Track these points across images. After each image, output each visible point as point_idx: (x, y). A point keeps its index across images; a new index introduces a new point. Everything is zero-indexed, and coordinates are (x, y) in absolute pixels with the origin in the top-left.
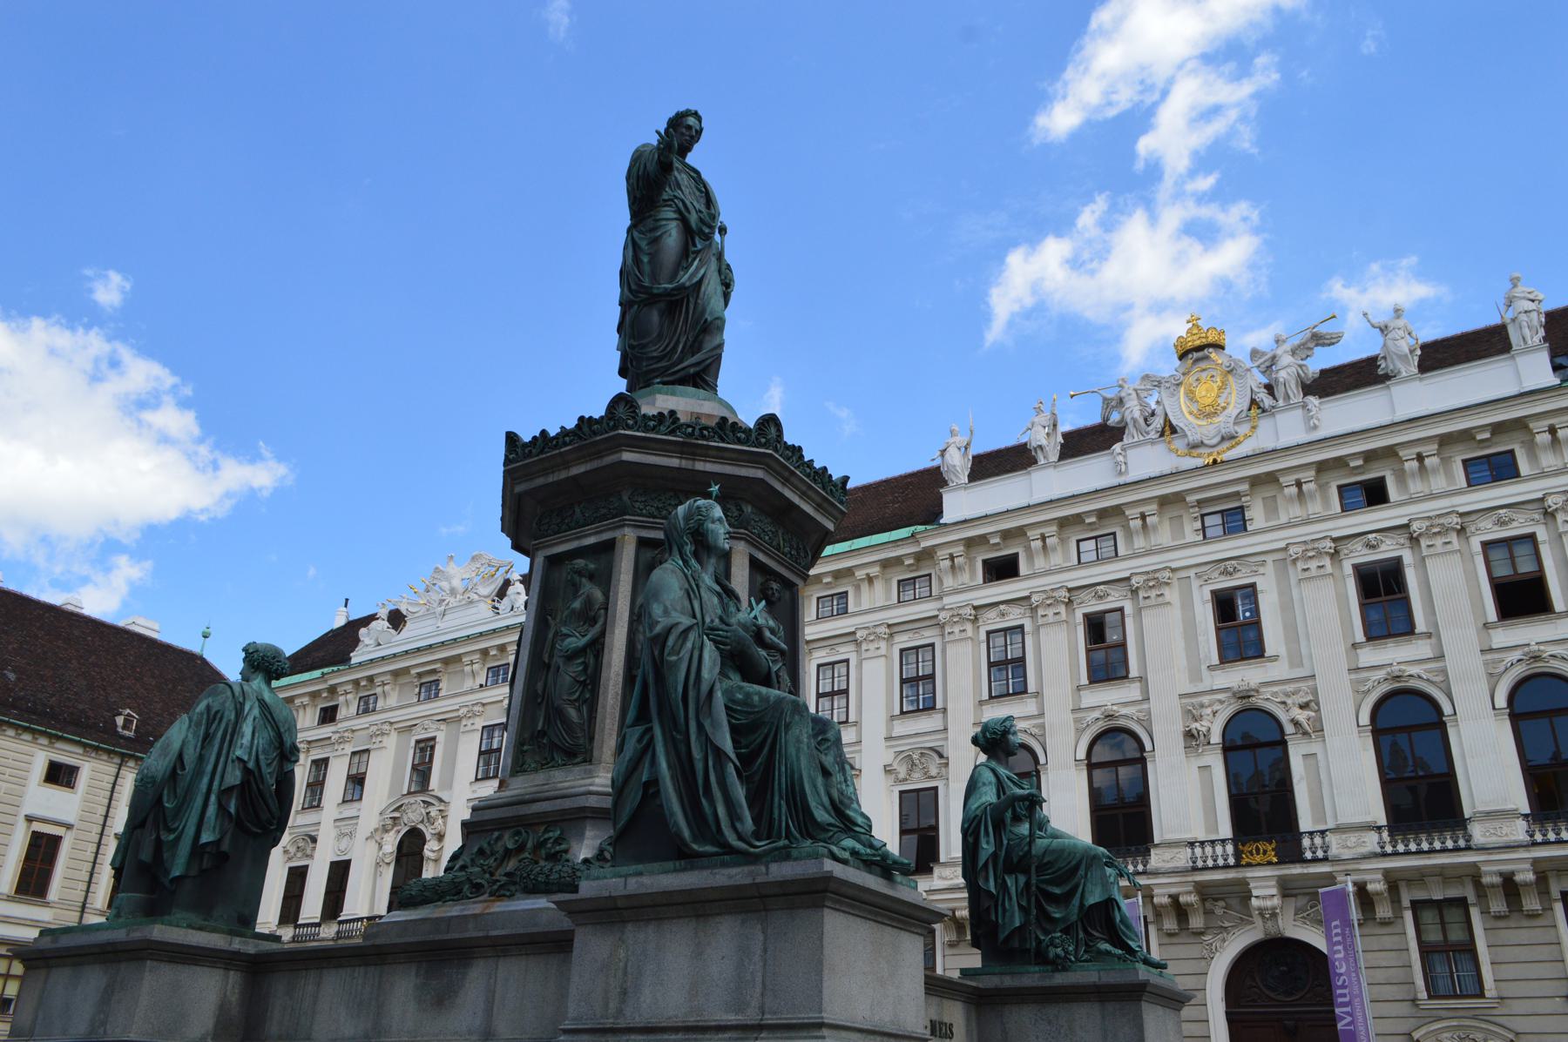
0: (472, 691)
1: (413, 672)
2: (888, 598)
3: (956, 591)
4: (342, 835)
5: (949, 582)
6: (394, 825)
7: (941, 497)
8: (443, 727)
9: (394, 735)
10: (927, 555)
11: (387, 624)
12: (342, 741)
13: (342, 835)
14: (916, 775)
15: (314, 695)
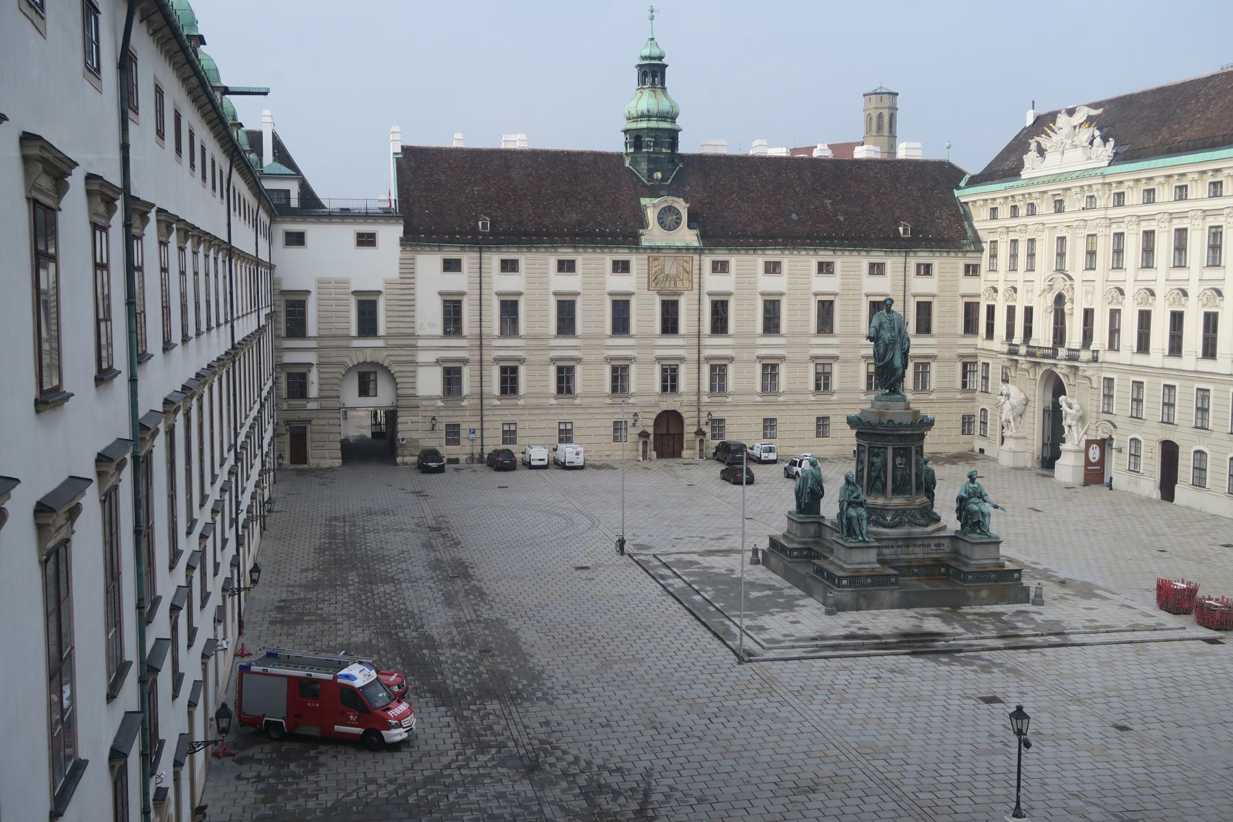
4: (1028, 291)
11: (1036, 154)
13: (1028, 291)
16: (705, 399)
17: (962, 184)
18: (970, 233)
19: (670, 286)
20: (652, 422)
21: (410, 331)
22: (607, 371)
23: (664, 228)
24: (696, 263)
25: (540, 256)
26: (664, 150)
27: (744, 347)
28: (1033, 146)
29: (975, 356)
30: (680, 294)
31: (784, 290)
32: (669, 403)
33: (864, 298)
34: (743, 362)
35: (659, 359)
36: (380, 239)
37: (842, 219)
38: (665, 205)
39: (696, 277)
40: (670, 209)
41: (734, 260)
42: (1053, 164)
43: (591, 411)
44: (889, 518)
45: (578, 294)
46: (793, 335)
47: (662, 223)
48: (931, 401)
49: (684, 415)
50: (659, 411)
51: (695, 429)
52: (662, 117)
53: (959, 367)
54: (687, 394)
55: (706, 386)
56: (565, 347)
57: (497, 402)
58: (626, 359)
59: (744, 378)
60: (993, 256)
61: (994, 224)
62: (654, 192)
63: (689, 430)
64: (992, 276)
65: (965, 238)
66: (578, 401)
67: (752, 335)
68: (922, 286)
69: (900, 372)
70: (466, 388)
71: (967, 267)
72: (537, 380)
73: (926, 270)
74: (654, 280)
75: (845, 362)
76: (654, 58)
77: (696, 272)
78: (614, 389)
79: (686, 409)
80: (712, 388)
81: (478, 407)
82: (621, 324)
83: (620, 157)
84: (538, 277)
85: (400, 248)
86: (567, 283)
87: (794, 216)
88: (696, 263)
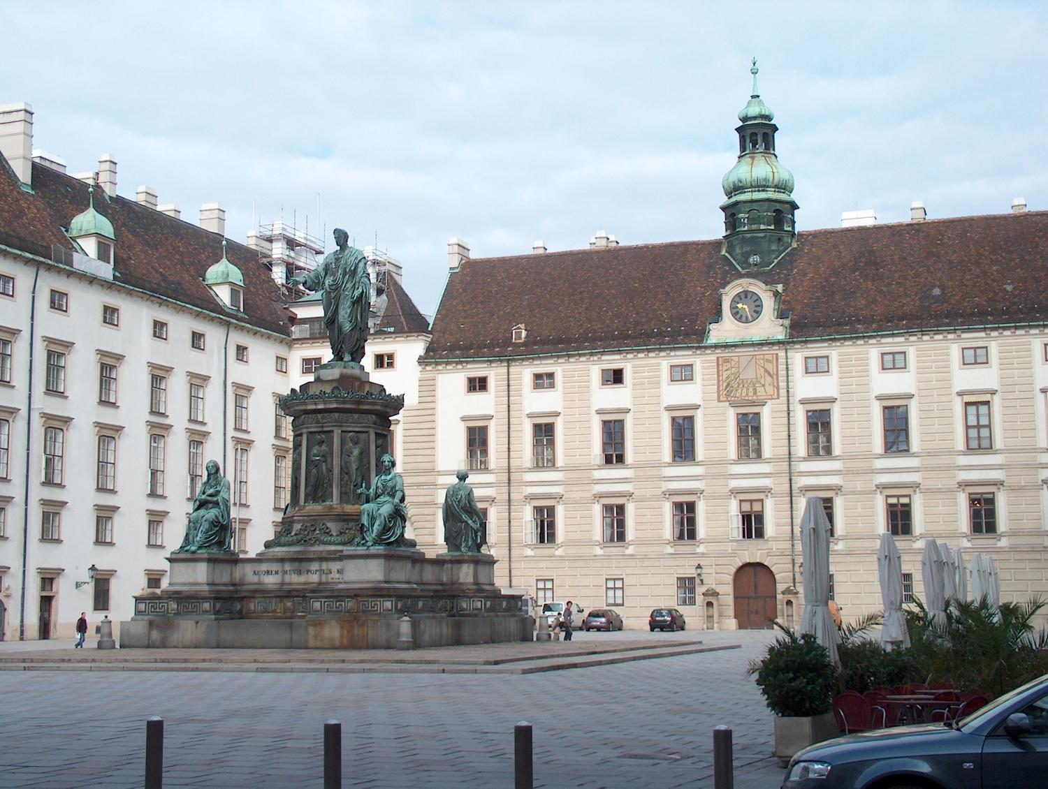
19: (741, 393)
21: (429, 466)
23: (739, 320)
24: (782, 361)
25: (579, 366)
26: (762, 227)
31: (912, 390)
32: (753, 552)
34: (854, 493)
35: (735, 492)
36: (398, 361)
37: (1009, 288)
38: (739, 290)
39: (782, 379)
40: (745, 295)
43: (646, 563)
44: (293, 534)
46: (930, 454)
47: (737, 315)
52: (761, 186)
54: (776, 539)
56: (613, 480)
57: (529, 552)
58: (690, 492)
66: (630, 551)
69: (347, 327)
76: (755, 118)
77: (782, 373)
79: (775, 559)
83: (717, 245)
85: (420, 368)
86: (615, 397)
87: (936, 291)
88: (782, 361)
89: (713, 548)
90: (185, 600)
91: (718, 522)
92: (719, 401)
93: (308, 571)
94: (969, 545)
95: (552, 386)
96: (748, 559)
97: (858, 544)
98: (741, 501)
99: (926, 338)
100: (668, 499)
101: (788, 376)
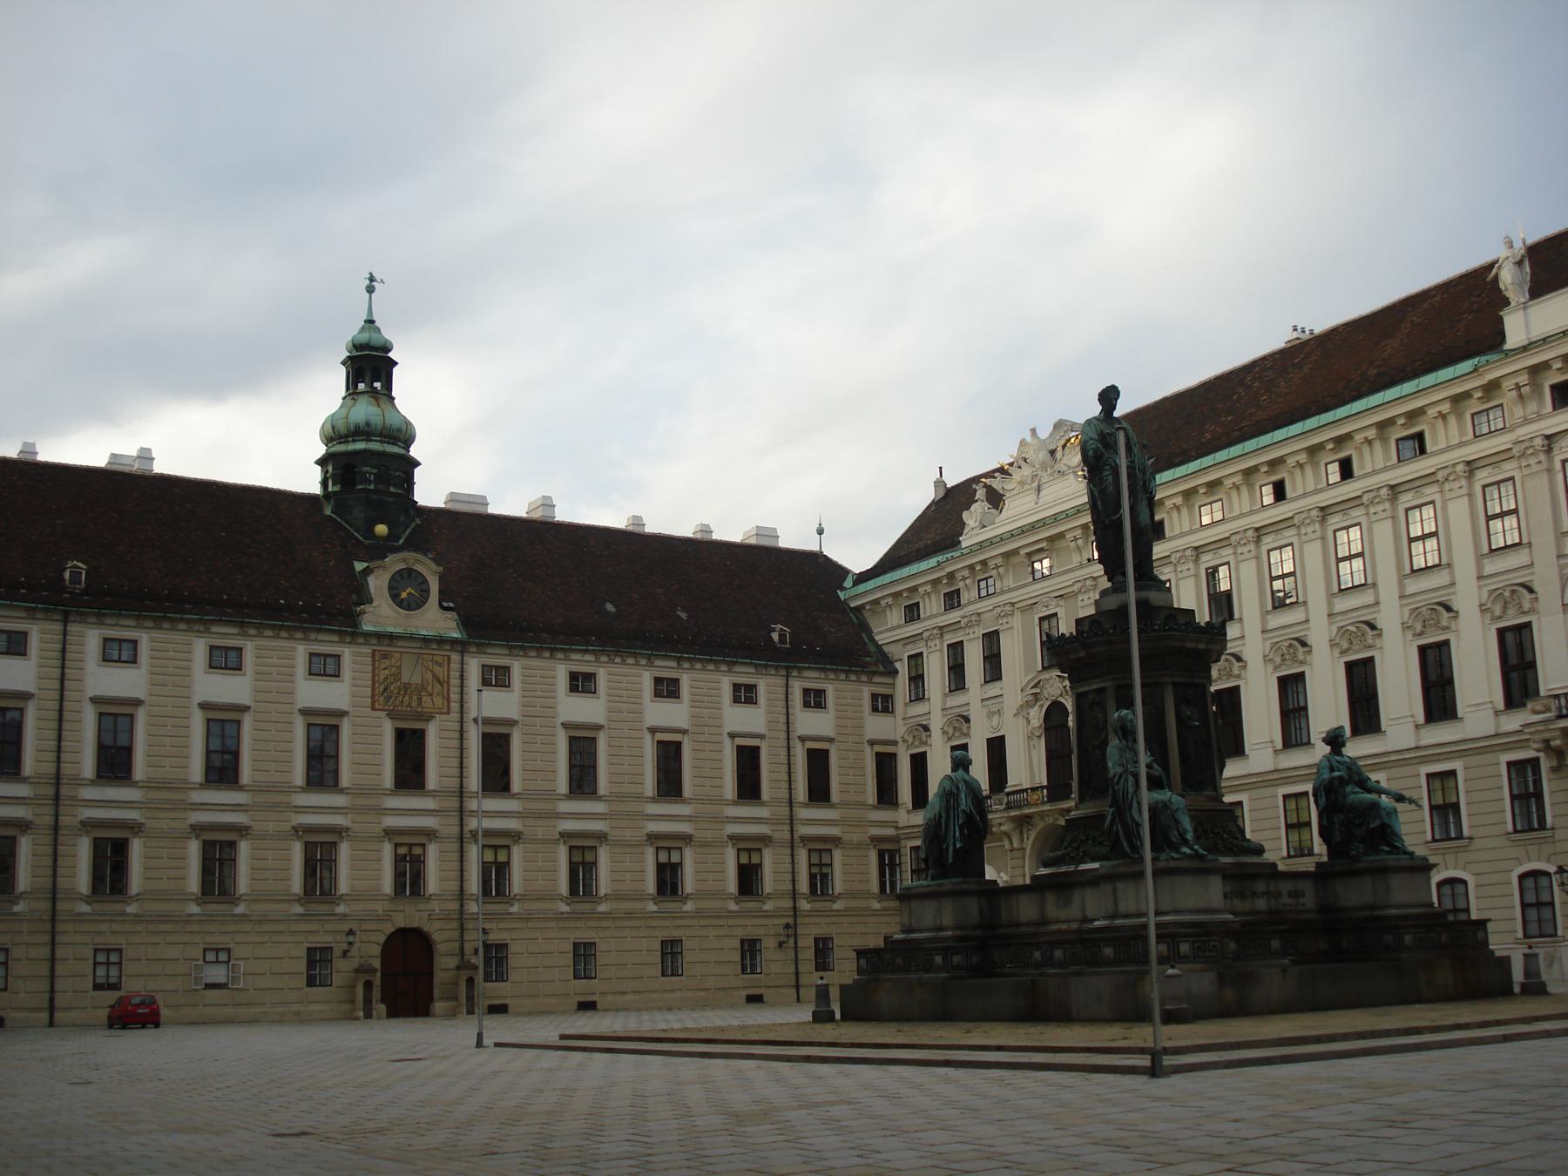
0: (1081, 566)
1: (1023, 552)
2: (1462, 432)
3: (1526, 421)
4: (990, 714)
5: (1519, 412)
6: (1037, 700)
7: (1501, 321)
8: (1062, 603)
9: (1018, 615)
10: (1492, 388)
12: (969, 625)
13: (990, 714)
14: (1511, 612)
15: (936, 582)
16: (472, 907)
17: (848, 583)
18: (872, 648)
20: (377, 950)
22: (297, 851)
24: (455, 666)
26: (392, 489)
27: (539, 816)
28: (980, 493)
29: (896, 839)
30: (429, 718)
31: (601, 721)
32: (409, 915)
33: (727, 741)
34: (536, 841)
37: (684, 615)
38: (402, 566)
40: (407, 575)
41: (517, 667)
42: (1019, 509)
43: (265, 927)
45: (246, 709)
47: (395, 596)
48: (838, 913)
49: (436, 937)
50: (389, 929)
51: (453, 962)
53: (873, 857)
55: (474, 885)
57: (85, 908)
59: (538, 871)
60: (917, 679)
61: (914, 628)
62: (379, 550)
63: (445, 965)
64: (919, 708)
65: (868, 654)
67: (551, 796)
68: (811, 723)
70: (23, 881)
71: (874, 696)
72: (163, 867)
73: (814, 699)
74: (385, 695)
75: (705, 844)
77: (455, 682)
78: (309, 890)
79: (438, 925)
80: (486, 891)
81: (47, 916)
82: (322, 766)
84: (171, 677)
87: (610, 607)
88: (455, 666)
89: (359, 907)
90: (1250, 935)
91: (364, 873)
92: (373, 709)
93: (1254, 894)
94: (654, 908)
95: (134, 660)
96: (401, 922)
97: (537, 906)
98: (397, 845)
99: (618, 660)
100: (299, 838)
101: (462, 686)
